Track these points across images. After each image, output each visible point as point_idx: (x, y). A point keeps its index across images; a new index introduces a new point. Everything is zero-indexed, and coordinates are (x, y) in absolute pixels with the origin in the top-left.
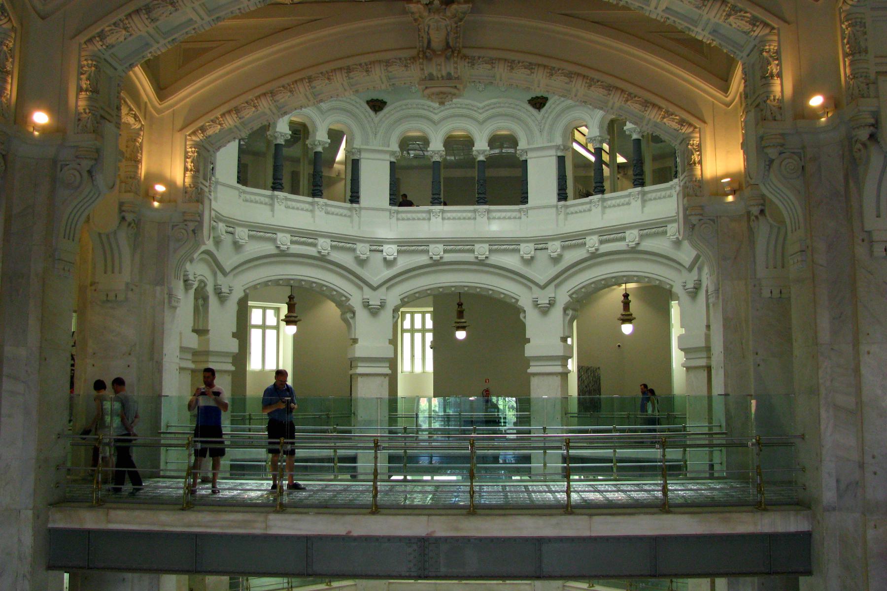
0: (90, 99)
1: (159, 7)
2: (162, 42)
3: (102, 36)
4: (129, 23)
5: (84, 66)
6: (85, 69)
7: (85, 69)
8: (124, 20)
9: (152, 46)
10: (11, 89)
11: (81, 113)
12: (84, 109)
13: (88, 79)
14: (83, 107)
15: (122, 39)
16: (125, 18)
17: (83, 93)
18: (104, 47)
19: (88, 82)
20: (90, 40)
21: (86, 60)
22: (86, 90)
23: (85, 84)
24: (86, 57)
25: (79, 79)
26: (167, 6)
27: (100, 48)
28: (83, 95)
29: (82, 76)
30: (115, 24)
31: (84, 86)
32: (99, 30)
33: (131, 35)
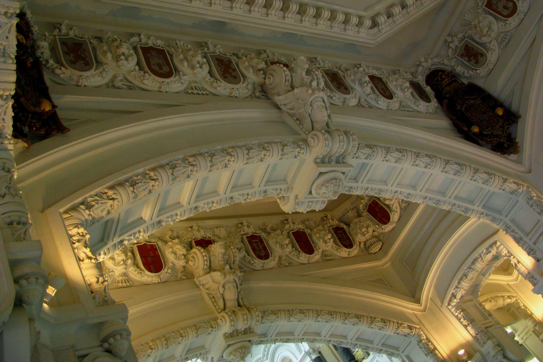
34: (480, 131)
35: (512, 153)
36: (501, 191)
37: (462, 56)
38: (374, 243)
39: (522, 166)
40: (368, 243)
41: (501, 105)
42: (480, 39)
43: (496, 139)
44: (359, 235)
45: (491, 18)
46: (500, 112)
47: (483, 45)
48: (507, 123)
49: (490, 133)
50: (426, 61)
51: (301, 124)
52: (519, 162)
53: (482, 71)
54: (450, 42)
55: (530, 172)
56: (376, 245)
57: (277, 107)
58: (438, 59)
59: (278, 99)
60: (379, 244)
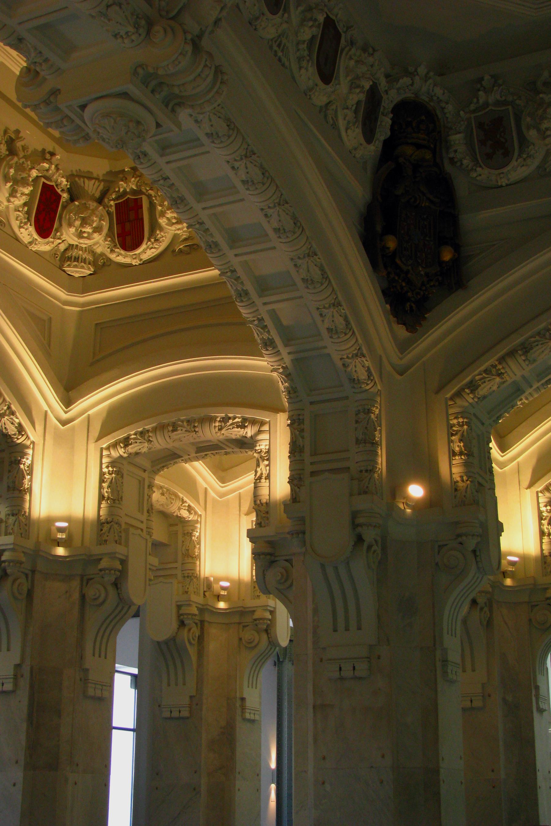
0: (466, 465)
1: (537, 345)
2: (536, 385)
3: (473, 386)
4: (503, 368)
5: (454, 425)
6: (454, 428)
7: (454, 428)
8: (496, 366)
9: (524, 392)
10: (382, 461)
11: (457, 482)
12: (461, 477)
13: (460, 441)
14: (460, 475)
15: (495, 388)
16: (497, 363)
17: (457, 458)
18: (476, 400)
19: (462, 444)
20: (459, 394)
21: (455, 418)
22: (461, 453)
23: (458, 446)
24: (455, 415)
25: (450, 442)
26: (547, 342)
27: (471, 401)
28: (457, 460)
29: (453, 438)
30: (485, 371)
31: (457, 449)
32: (468, 379)
33: (504, 382)
35: (404, 324)
36: (339, 364)
37: (480, 126)
38: (84, 261)
40: (75, 253)
41: (457, 248)
42: (528, 128)
43: (404, 284)
46: (447, 255)
47: (523, 141)
48: (440, 279)
50: (426, 78)
54: (485, 88)
55: (401, 374)
56: (82, 267)
58: (444, 94)
60: (89, 269)
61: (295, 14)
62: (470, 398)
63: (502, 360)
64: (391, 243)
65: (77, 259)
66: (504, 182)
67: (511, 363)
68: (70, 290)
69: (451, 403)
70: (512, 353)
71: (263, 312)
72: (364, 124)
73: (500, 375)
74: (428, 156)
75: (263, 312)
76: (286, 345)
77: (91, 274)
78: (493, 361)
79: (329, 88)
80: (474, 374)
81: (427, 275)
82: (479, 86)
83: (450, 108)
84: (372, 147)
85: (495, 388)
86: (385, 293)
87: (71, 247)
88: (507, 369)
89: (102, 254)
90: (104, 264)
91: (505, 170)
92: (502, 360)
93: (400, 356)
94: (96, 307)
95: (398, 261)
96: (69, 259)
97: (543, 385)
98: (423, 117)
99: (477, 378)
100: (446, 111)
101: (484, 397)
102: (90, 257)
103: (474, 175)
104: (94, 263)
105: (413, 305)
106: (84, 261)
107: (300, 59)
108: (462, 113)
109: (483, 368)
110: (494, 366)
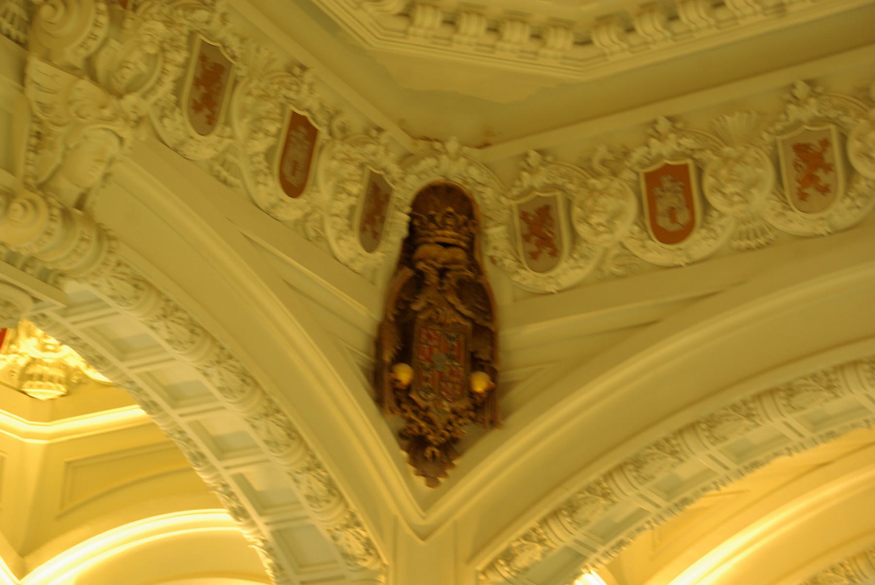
2: (602, 549)
3: (508, 556)
4: (546, 533)
15: (538, 558)
20: (492, 567)
27: (506, 575)
34: (409, 388)
35: (424, 476)
36: (327, 536)
37: (524, 216)
38: (51, 379)
39: (421, 512)
40: (37, 369)
41: (493, 374)
44: (33, 341)
45: (631, 206)
46: (480, 383)
49: (422, 404)
51: (35, 150)
52: (426, 505)
53: (528, 278)
55: (424, 538)
56: (49, 388)
57: (22, 76)
59: (37, 68)
60: (58, 389)
61: (241, 128)
62: (505, 571)
63: (544, 522)
64: (404, 374)
65: (41, 377)
66: (552, 288)
67: (553, 524)
68: (33, 417)
69: (482, 577)
70: (555, 514)
71: (227, 477)
72: (363, 230)
73: (541, 541)
74: (461, 255)
75: (227, 477)
76: (261, 514)
77: (63, 396)
78: (533, 523)
79: (301, 201)
80: (510, 540)
81: (454, 412)
82: (523, 164)
83: (489, 193)
84: (378, 255)
85: (538, 558)
86: (401, 435)
87: (33, 361)
88: (551, 535)
89: (77, 369)
90: (80, 383)
91: (552, 273)
92: (544, 522)
93: (424, 514)
94: (70, 440)
95: (414, 396)
96: (31, 377)
97: (613, 548)
98: (451, 210)
99: (515, 545)
100: (484, 196)
101: (526, 569)
102: (60, 374)
103: (516, 278)
104: (67, 382)
105: (436, 450)
106: (51, 379)
107: (256, 173)
108: (503, 199)
109: (521, 531)
110: (534, 530)
